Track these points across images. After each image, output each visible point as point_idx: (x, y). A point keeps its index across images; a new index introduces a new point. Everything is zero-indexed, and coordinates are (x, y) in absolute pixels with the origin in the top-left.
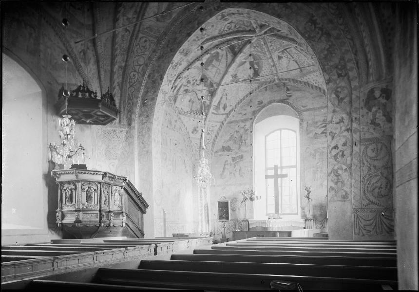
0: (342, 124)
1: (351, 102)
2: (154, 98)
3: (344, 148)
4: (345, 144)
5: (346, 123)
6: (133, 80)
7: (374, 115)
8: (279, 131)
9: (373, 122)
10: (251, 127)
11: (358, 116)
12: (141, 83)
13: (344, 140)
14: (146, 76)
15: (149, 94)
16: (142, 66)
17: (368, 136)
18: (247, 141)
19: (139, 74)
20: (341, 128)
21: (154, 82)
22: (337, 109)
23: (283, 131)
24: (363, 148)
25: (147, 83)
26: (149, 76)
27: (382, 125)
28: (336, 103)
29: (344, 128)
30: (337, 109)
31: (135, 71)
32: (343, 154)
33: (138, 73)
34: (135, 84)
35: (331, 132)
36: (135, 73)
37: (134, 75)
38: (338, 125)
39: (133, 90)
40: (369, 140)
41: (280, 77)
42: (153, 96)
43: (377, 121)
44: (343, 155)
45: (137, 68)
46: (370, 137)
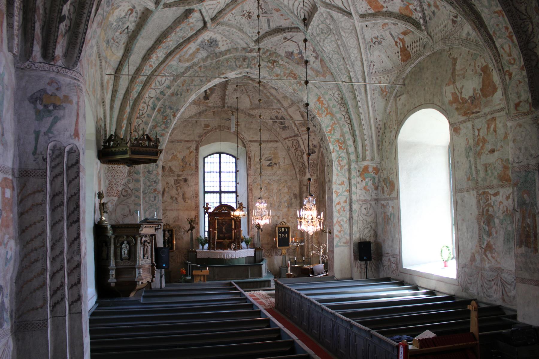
0: (343, 186)
1: (349, 170)
2: (164, 134)
3: (344, 205)
4: (345, 202)
5: (346, 186)
6: (141, 112)
7: (367, 183)
8: (218, 155)
9: (365, 188)
10: (197, 149)
11: (355, 182)
12: (149, 116)
13: (344, 199)
14: (156, 110)
15: (158, 129)
16: (152, 100)
17: (362, 198)
18: (191, 164)
19: (149, 107)
20: (343, 188)
21: (166, 117)
22: (340, 174)
23: (222, 155)
24: (359, 206)
25: (156, 116)
26: (159, 110)
27: (371, 191)
28: (339, 168)
29: (344, 189)
30: (340, 174)
31: (145, 103)
32: (344, 209)
33: (148, 105)
34: (143, 116)
35: (336, 191)
36: (145, 105)
37: (143, 107)
38: (340, 187)
39: (140, 122)
40: (362, 201)
41: (229, 105)
42: (163, 132)
43: (368, 188)
44: (344, 210)
45: (147, 100)
46: (363, 198)
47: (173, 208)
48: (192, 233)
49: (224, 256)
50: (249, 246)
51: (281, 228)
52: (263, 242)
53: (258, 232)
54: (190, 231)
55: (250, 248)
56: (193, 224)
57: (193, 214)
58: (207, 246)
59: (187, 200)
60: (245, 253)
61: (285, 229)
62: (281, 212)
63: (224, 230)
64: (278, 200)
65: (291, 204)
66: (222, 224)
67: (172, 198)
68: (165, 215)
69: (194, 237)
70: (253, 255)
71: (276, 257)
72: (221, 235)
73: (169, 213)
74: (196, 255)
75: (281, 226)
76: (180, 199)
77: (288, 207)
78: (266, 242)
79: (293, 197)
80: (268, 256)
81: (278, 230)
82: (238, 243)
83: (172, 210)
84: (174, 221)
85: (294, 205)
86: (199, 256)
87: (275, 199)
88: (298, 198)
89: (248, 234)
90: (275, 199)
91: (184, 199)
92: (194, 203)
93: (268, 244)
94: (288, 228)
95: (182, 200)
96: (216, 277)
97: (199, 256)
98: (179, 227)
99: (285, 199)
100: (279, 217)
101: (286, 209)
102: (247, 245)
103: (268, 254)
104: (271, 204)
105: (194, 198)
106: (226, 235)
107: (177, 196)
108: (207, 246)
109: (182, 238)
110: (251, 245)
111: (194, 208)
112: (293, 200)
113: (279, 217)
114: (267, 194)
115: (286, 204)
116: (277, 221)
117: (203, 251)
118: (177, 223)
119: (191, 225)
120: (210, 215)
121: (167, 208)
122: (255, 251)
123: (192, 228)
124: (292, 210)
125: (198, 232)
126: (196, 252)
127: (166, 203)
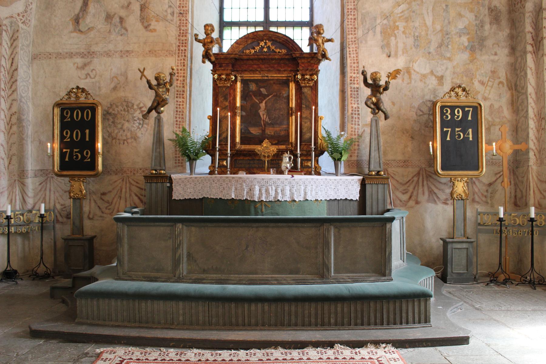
47: (111, 47)
48: (159, 120)
49: (251, 190)
50: (342, 169)
51: (453, 108)
52: (390, 157)
53: (375, 123)
54: (154, 114)
55: (345, 174)
56: (161, 90)
57: (169, 63)
58: (204, 163)
59: (154, 24)
60: (328, 188)
61: (465, 114)
62: (450, 65)
63: (262, 113)
64: (438, 27)
65: (482, 41)
66: (258, 94)
67: (109, 17)
68: (87, 69)
69: (168, 133)
70: (355, 195)
71: (430, 205)
72: (255, 131)
73: (98, 64)
74: (171, 189)
75: (452, 100)
76: (133, 20)
77: (472, 49)
78: (400, 157)
79: (487, 20)
80: (404, 204)
81: (442, 114)
82: (306, 155)
83: (108, 54)
84: (115, 89)
85: (489, 43)
86: (178, 194)
87: (429, 21)
88: (504, 22)
89: (343, 127)
90: (429, 21)
91: (145, 21)
92: (173, 32)
93: (405, 163)
94: (477, 109)
95: (139, 25)
96: (184, 268)
97: (178, 194)
98: (128, 106)
99: (461, 26)
100: (441, 79)
101: (465, 56)
102: (337, 161)
103: (405, 197)
104: (417, 38)
105: (176, 19)
106: (270, 131)
107: (123, 13)
108: (204, 163)
109: (135, 138)
110: (349, 164)
111: (174, 48)
112: (487, 27)
113: (441, 79)
114: (403, 7)
115: (464, 40)
116: (434, 91)
117: (197, 179)
118: (121, 94)
119: (157, 95)
120: (221, 63)
121: (94, 48)
122: (363, 185)
123: (158, 104)
124: (485, 57)
125: (181, 115)
126: (170, 180)
127: (92, 34)
